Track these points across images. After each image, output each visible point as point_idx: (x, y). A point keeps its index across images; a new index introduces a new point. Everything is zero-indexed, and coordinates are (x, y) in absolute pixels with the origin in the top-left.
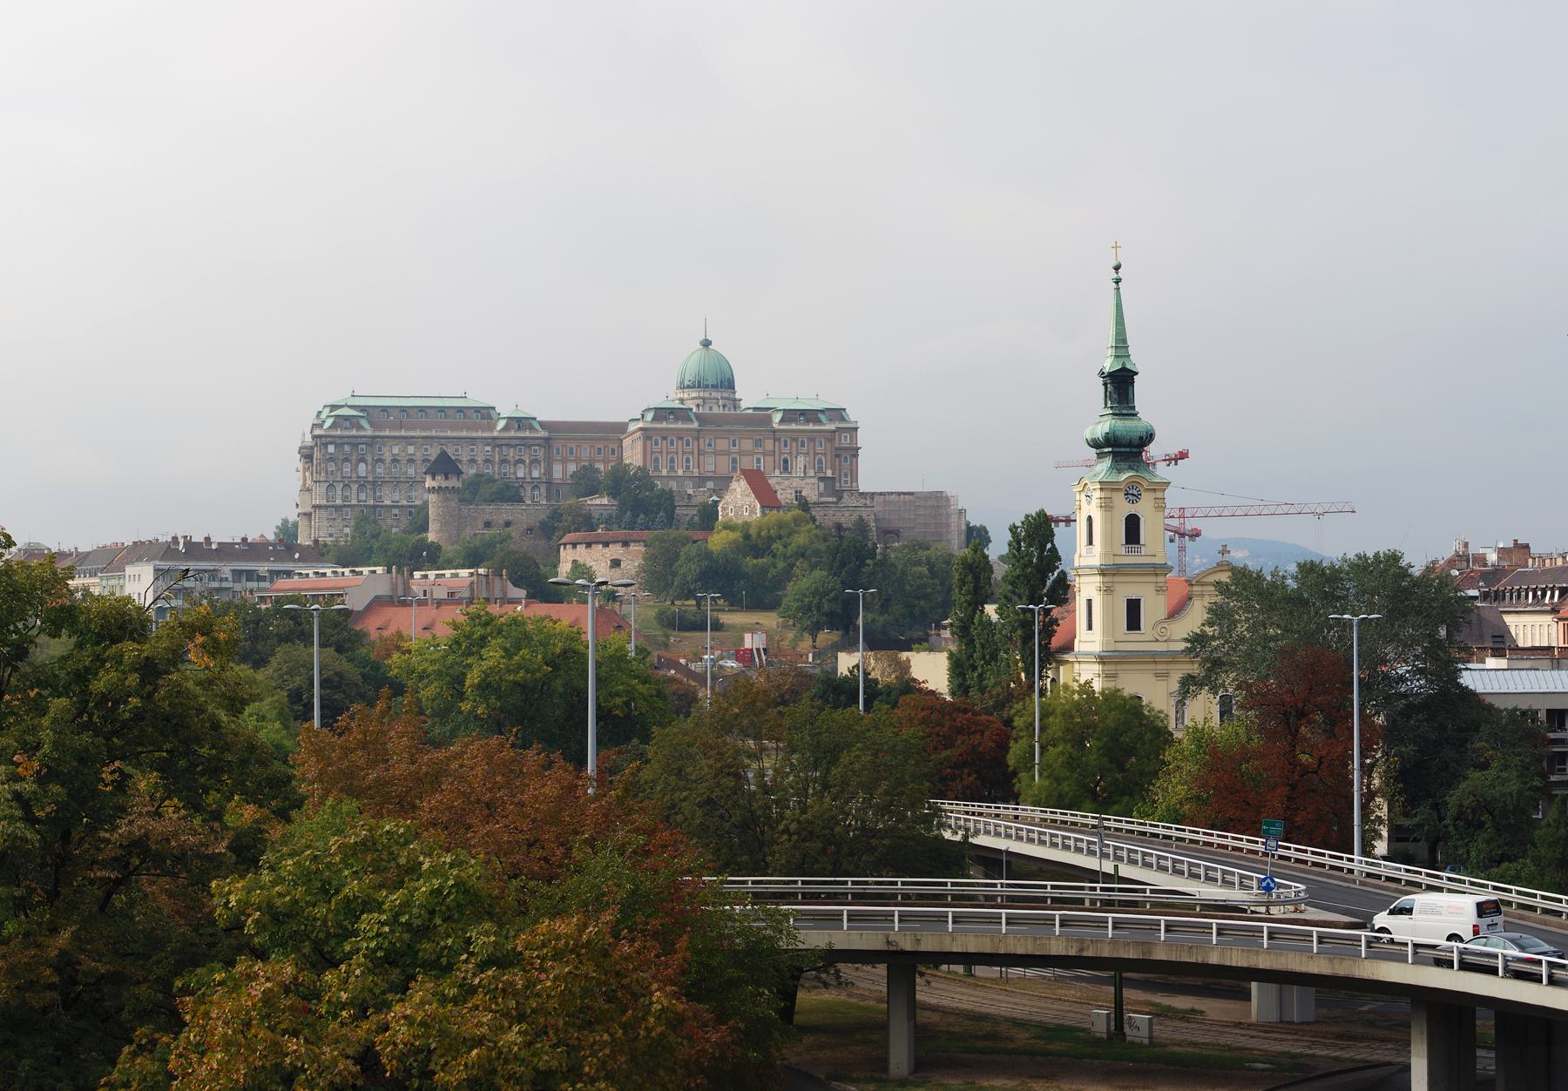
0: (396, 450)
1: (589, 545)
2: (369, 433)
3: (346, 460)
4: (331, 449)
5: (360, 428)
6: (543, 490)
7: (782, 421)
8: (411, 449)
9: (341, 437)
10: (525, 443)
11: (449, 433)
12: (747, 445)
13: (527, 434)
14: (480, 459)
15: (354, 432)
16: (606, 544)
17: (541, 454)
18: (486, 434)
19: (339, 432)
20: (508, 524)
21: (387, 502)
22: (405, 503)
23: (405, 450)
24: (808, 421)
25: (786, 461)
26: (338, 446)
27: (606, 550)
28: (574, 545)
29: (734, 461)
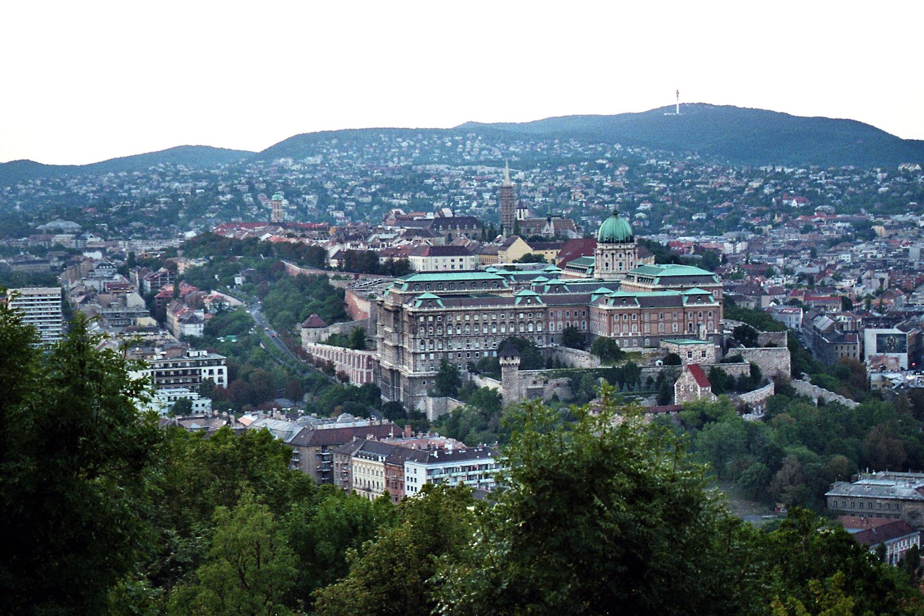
0: (458, 318)
2: (444, 309)
3: (430, 325)
4: (422, 319)
5: (438, 306)
6: (544, 339)
8: (467, 318)
9: (427, 312)
10: (533, 311)
11: (490, 307)
13: (535, 306)
14: (507, 322)
15: (435, 309)
18: (510, 307)
19: (426, 310)
23: (464, 318)
24: (703, 302)
25: (690, 325)
26: (426, 318)
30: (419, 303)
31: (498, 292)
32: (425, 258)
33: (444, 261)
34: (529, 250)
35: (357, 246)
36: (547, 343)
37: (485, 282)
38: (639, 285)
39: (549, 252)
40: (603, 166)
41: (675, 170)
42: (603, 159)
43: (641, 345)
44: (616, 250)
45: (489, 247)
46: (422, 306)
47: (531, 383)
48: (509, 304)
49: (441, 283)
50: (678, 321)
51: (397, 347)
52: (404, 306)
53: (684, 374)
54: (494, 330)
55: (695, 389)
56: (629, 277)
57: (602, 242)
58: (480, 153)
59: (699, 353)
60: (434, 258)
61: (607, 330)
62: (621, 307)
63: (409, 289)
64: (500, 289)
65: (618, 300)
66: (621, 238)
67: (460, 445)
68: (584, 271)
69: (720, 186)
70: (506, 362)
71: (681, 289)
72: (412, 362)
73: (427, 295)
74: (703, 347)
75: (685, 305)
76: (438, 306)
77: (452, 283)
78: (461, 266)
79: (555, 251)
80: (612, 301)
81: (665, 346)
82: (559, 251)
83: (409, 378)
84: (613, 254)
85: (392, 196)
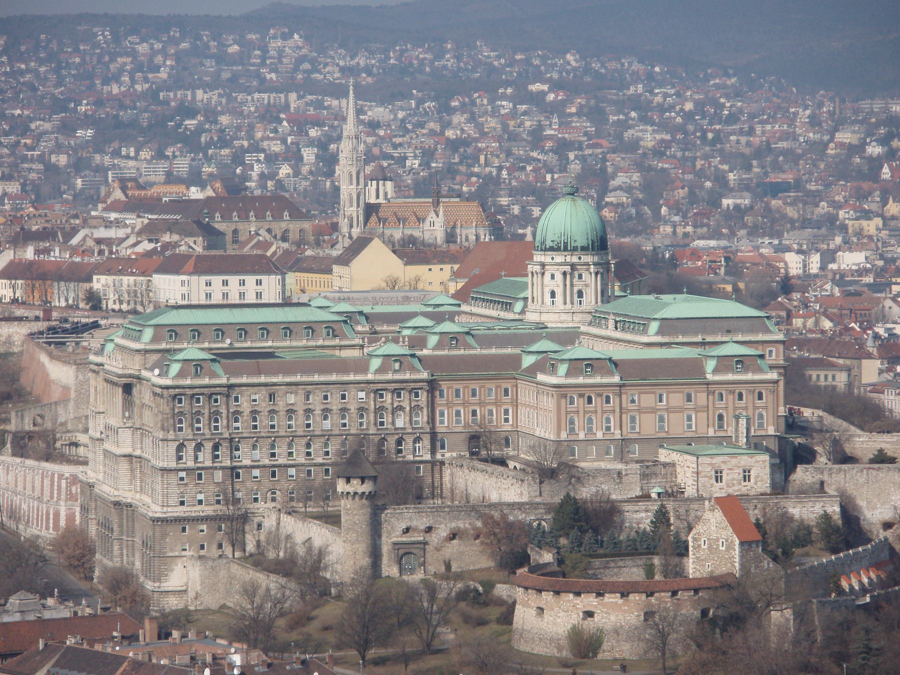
1: (557, 593)
2: (224, 381)
7: (716, 371)
9: (191, 387)
11: (316, 378)
12: (676, 399)
14: (353, 407)
15: (206, 381)
16: (578, 594)
17: (423, 397)
18: (359, 377)
19: (188, 382)
20: (429, 530)
21: (246, 462)
22: (266, 462)
24: (746, 370)
25: (721, 417)
27: (578, 600)
28: (540, 591)
29: (662, 419)
30: (175, 368)
31: (334, 347)
32: (184, 278)
33: (225, 283)
34: (394, 266)
35: (47, 251)
36: (433, 451)
37: (310, 328)
38: (618, 335)
39: (436, 268)
40: (543, 94)
41: (689, 106)
42: (543, 82)
43: (622, 456)
44: (573, 266)
45: (314, 258)
46: (181, 374)
47: (399, 531)
48: (356, 372)
49: (220, 330)
50: (696, 410)
51: (129, 456)
52: (145, 374)
53: (708, 515)
54: (327, 425)
55: (730, 547)
56: (597, 319)
57: (545, 250)
58: (296, 69)
59: (738, 474)
60: (204, 278)
61: (553, 426)
62: (580, 380)
63: (155, 339)
64: (337, 341)
65: (578, 366)
66: (579, 244)
67: (256, 657)
68: (508, 306)
69: (781, 139)
70: (349, 488)
71: (703, 344)
72: (159, 488)
73: (193, 351)
74: (745, 461)
75: (710, 377)
76: (213, 375)
77: (243, 330)
78: (259, 295)
79: (447, 268)
80: (563, 369)
81: (667, 460)
82: (456, 267)
83: (155, 520)
84: (565, 274)
85: (116, 153)
